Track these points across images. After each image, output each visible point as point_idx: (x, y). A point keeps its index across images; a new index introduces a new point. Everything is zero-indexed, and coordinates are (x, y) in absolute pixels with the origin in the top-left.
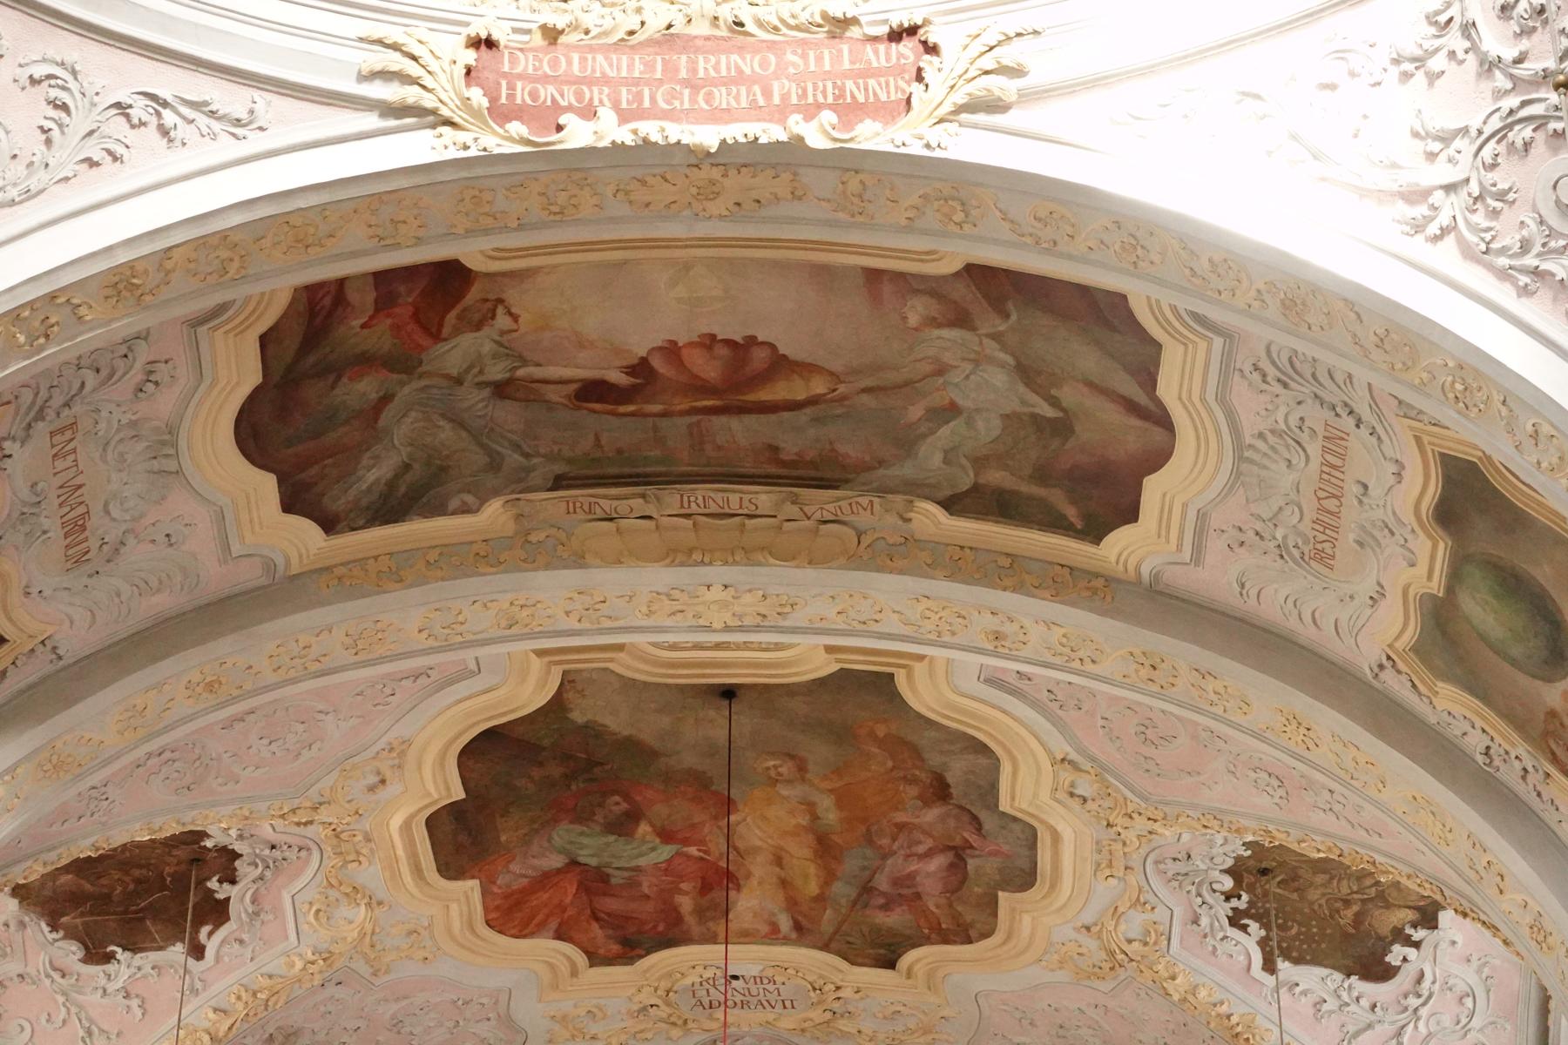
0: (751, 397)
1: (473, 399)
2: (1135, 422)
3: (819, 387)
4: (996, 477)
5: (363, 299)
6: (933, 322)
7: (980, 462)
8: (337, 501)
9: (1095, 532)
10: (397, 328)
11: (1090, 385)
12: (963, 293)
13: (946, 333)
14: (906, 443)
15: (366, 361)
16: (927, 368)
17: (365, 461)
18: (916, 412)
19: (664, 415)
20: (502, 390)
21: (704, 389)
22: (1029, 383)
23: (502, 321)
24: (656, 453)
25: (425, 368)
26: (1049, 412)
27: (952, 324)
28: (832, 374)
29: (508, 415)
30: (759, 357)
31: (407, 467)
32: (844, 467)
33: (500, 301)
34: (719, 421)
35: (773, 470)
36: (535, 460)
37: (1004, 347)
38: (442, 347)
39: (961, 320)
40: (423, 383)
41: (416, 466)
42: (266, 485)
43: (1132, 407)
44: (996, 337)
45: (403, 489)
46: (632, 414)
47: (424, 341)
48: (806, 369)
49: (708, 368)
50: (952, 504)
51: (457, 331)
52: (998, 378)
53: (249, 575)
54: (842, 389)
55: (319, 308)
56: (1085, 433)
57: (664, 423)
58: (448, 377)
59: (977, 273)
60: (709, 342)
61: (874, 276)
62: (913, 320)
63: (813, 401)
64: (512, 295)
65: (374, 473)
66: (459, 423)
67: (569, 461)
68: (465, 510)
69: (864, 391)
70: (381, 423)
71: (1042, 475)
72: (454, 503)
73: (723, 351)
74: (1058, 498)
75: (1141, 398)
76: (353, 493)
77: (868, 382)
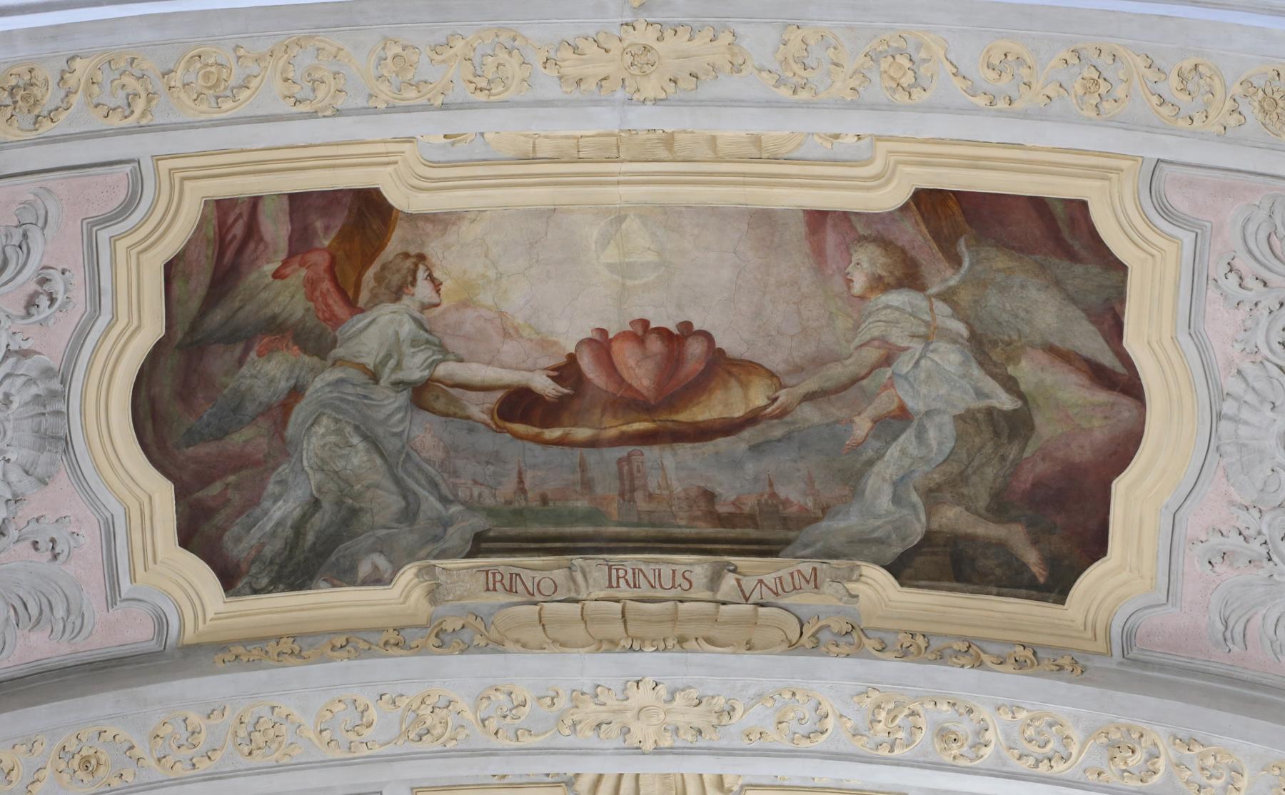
0: (684, 417)
1: (391, 403)
2: (1102, 396)
3: (758, 396)
4: (952, 517)
5: (276, 230)
6: (879, 284)
7: (933, 496)
8: (240, 546)
9: (1056, 587)
10: (311, 284)
11: (1052, 350)
12: (913, 235)
13: (897, 298)
14: (852, 478)
15: (276, 330)
16: (872, 354)
17: (272, 488)
18: (862, 426)
19: (592, 444)
20: (421, 395)
21: (631, 403)
22: (985, 362)
23: (423, 290)
24: (582, 504)
25: (339, 352)
26: (1005, 402)
27: (900, 284)
28: (772, 375)
29: (425, 434)
30: (695, 349)
31: (316, 504)
32: (785, 522)
33: (421, 258)
34: (651, 454)
35: (708, 530)
36: (454, 509)
37: (957, 312)
38: (360, 321)
39: (910, 278)
40: (337, 374)
41: (326, 505)
42: (162, 492)
43: (1100, 375)
44: (947, 297)
45: (310, 538)
46: (559, 442)
47: (339, 309)
48: (743, 369)
49: (640, 371)
50: (902, 569)
51: (375, 301)
52: (950, 358)
53: (135, 633)
54: (783, 396)
55: (231, 232)
56: (1046, 427)
57: (592, 456)
58: (363, 368)
59: (927, 202)
60: (642, 331)
61: (817, 219)
62: (859, 282)
63: (752, 419)
64: (433, 250)
65: (281, 509)
66: (374, 443)
67: (491, 513)
68: (377, 580)
69: (809, 397)
70: (291, 430)
71: (1000, 508)
72: (364, 569)
73: (655, 345)
74: (1015, 535)
75: (1107, 359)
76: (256, 533)
77: (811, 385)
